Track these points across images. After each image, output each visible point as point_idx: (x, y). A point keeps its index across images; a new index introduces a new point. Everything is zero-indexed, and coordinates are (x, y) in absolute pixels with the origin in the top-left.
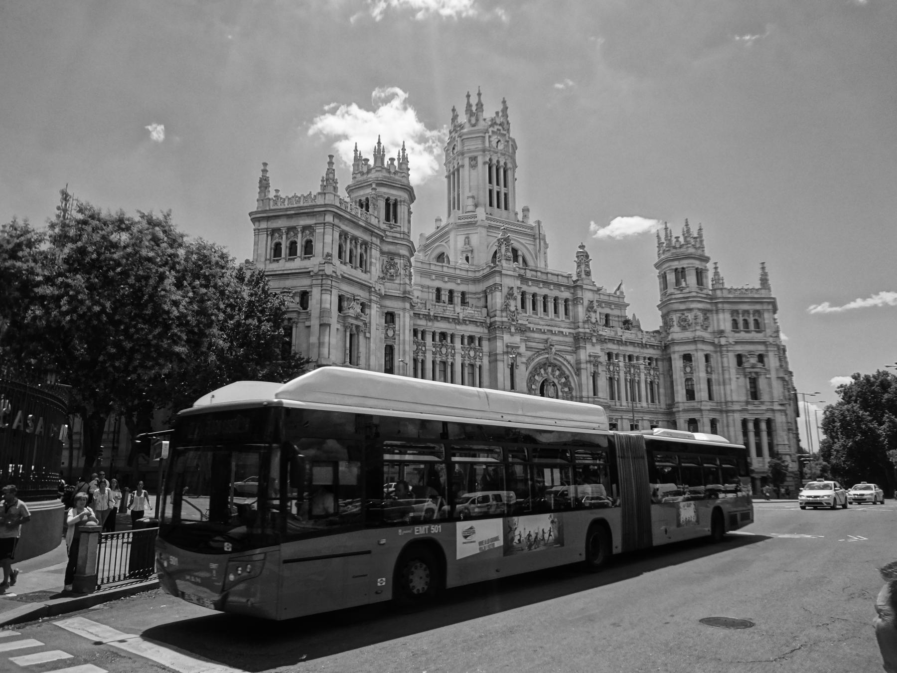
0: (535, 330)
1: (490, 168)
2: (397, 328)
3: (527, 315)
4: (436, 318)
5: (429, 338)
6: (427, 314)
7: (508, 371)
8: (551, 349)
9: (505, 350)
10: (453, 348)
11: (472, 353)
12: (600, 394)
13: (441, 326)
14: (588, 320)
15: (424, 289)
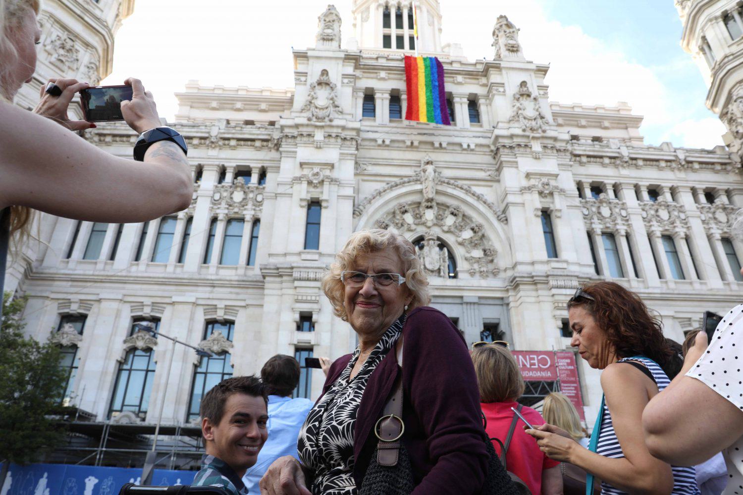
0: (387, 142)
3: (377, 123)
7: (301, 215)
8: (424, 171)
11: (238, 196)
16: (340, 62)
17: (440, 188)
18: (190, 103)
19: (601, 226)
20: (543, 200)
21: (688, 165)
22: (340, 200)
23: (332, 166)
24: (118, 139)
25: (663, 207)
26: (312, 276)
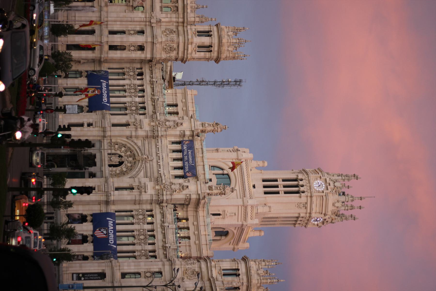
1: (296, 180)
2: (135, 35)
4: (152, 83)
5: (139, 82)
6: (154, 77)
9: (137, 119)
10: (135, 96)
11: (134, 108)
12: (116, 192)
13: (148, 89)
14: (173, 184)
15: (174, 97)
16: (190, 129)
17: (141, 161)
18: (183, 93)
19: (134, 214)
20: (137, 187)
21: (165, 248)
22: (130, 132)
23: (141, 128)
24: (151, 72)
25: (145, 237)
26: (103, 124)
